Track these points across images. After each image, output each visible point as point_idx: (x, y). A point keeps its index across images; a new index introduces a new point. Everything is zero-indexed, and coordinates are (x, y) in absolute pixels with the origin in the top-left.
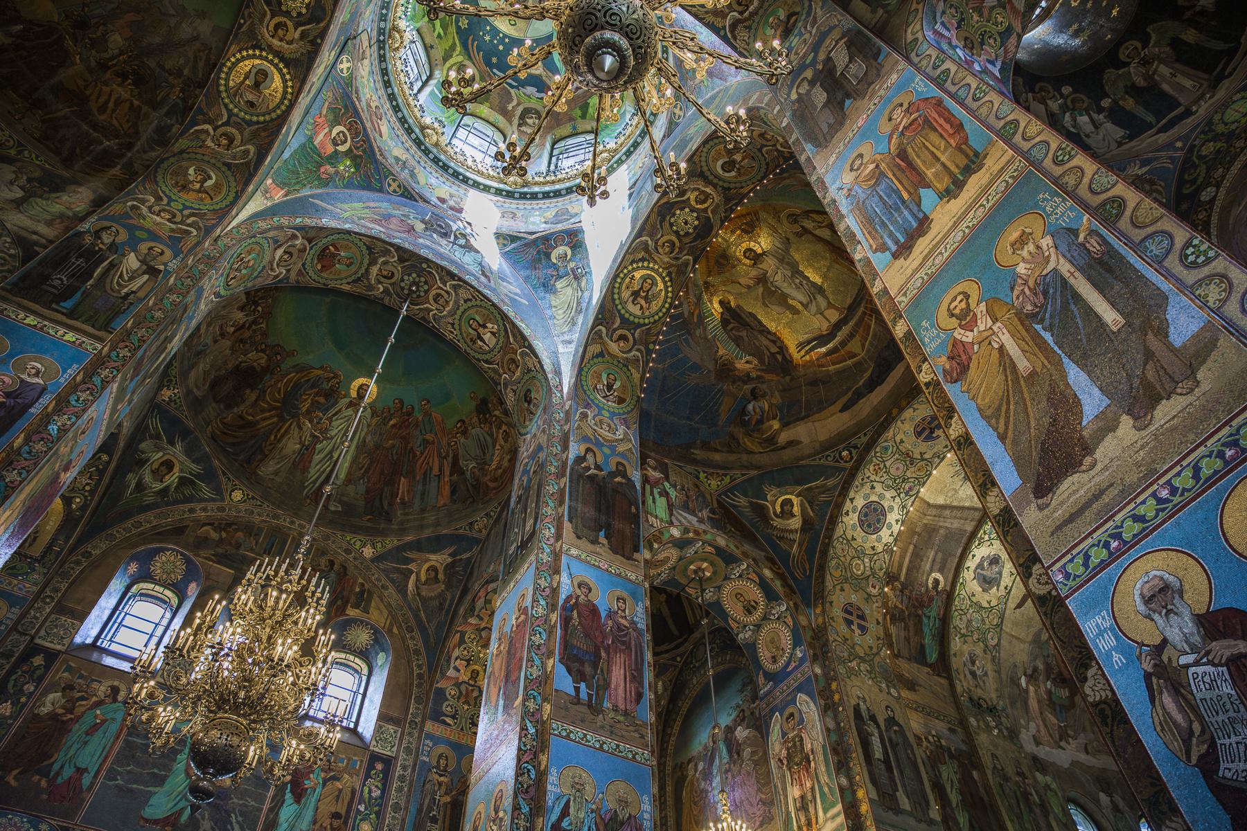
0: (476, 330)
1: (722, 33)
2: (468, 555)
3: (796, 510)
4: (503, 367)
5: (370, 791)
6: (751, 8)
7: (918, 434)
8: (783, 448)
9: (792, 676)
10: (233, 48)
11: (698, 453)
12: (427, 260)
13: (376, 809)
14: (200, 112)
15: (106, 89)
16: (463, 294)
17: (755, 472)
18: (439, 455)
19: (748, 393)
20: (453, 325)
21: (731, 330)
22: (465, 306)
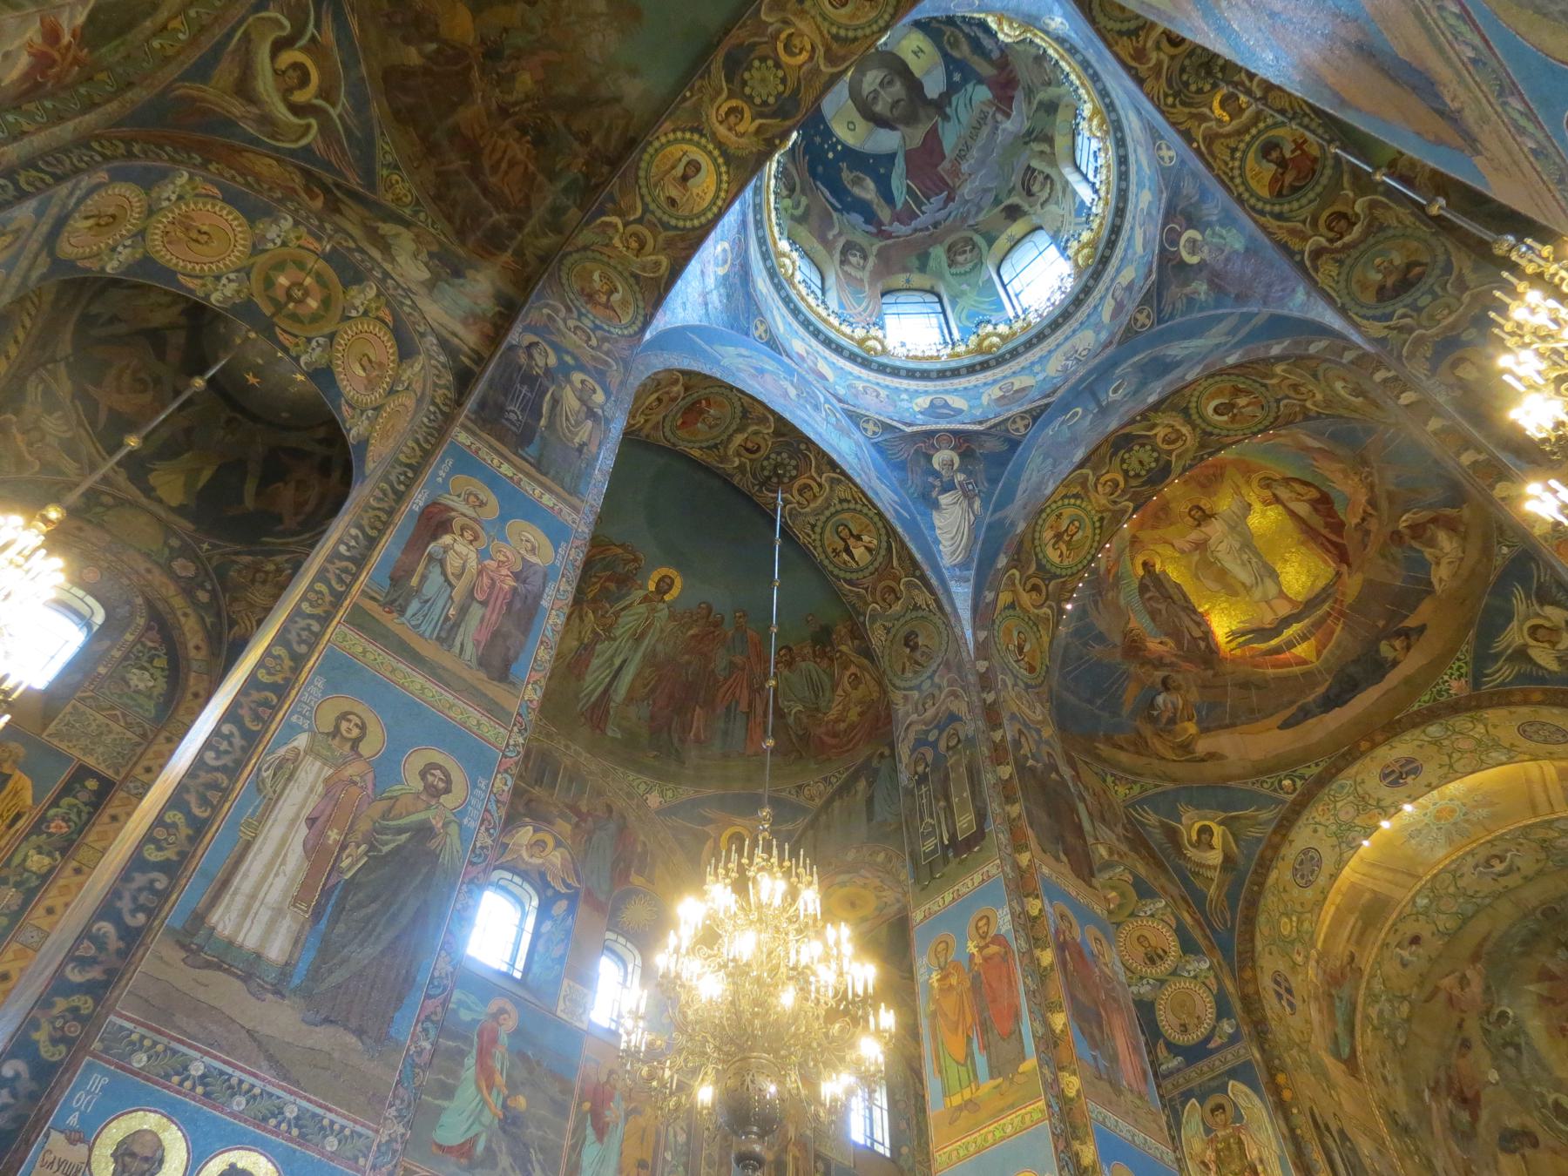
0: (844, 540)
1: (1298, 258)
2: (790, 827)
3: (1217, 841)
4: (873, 594)
5: (675, 1136)
6: (1347, 239)
7: (1385, 776)
8: (1202, 760)
9: (1215, 1057)
10: (668, 125)
11: (1104, 749)
12: (808, 441)
13: (684, 1159)
14: (611, 198)
15: (502, 143)
16: (841, 491)
17: (1169, 786)
18: (750, 686)
19: (1158, 680)
20: (813, 527)
21: (1150, 599)
22: (839, 507)
